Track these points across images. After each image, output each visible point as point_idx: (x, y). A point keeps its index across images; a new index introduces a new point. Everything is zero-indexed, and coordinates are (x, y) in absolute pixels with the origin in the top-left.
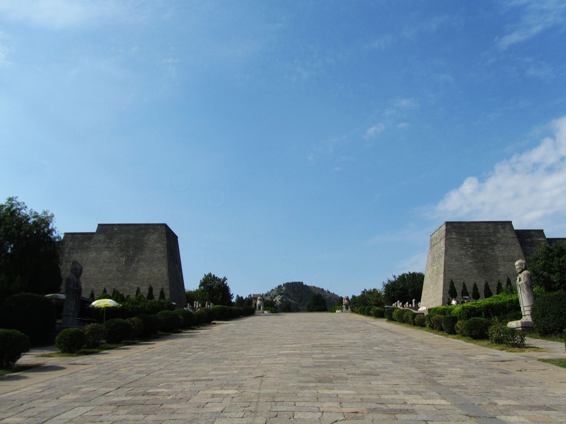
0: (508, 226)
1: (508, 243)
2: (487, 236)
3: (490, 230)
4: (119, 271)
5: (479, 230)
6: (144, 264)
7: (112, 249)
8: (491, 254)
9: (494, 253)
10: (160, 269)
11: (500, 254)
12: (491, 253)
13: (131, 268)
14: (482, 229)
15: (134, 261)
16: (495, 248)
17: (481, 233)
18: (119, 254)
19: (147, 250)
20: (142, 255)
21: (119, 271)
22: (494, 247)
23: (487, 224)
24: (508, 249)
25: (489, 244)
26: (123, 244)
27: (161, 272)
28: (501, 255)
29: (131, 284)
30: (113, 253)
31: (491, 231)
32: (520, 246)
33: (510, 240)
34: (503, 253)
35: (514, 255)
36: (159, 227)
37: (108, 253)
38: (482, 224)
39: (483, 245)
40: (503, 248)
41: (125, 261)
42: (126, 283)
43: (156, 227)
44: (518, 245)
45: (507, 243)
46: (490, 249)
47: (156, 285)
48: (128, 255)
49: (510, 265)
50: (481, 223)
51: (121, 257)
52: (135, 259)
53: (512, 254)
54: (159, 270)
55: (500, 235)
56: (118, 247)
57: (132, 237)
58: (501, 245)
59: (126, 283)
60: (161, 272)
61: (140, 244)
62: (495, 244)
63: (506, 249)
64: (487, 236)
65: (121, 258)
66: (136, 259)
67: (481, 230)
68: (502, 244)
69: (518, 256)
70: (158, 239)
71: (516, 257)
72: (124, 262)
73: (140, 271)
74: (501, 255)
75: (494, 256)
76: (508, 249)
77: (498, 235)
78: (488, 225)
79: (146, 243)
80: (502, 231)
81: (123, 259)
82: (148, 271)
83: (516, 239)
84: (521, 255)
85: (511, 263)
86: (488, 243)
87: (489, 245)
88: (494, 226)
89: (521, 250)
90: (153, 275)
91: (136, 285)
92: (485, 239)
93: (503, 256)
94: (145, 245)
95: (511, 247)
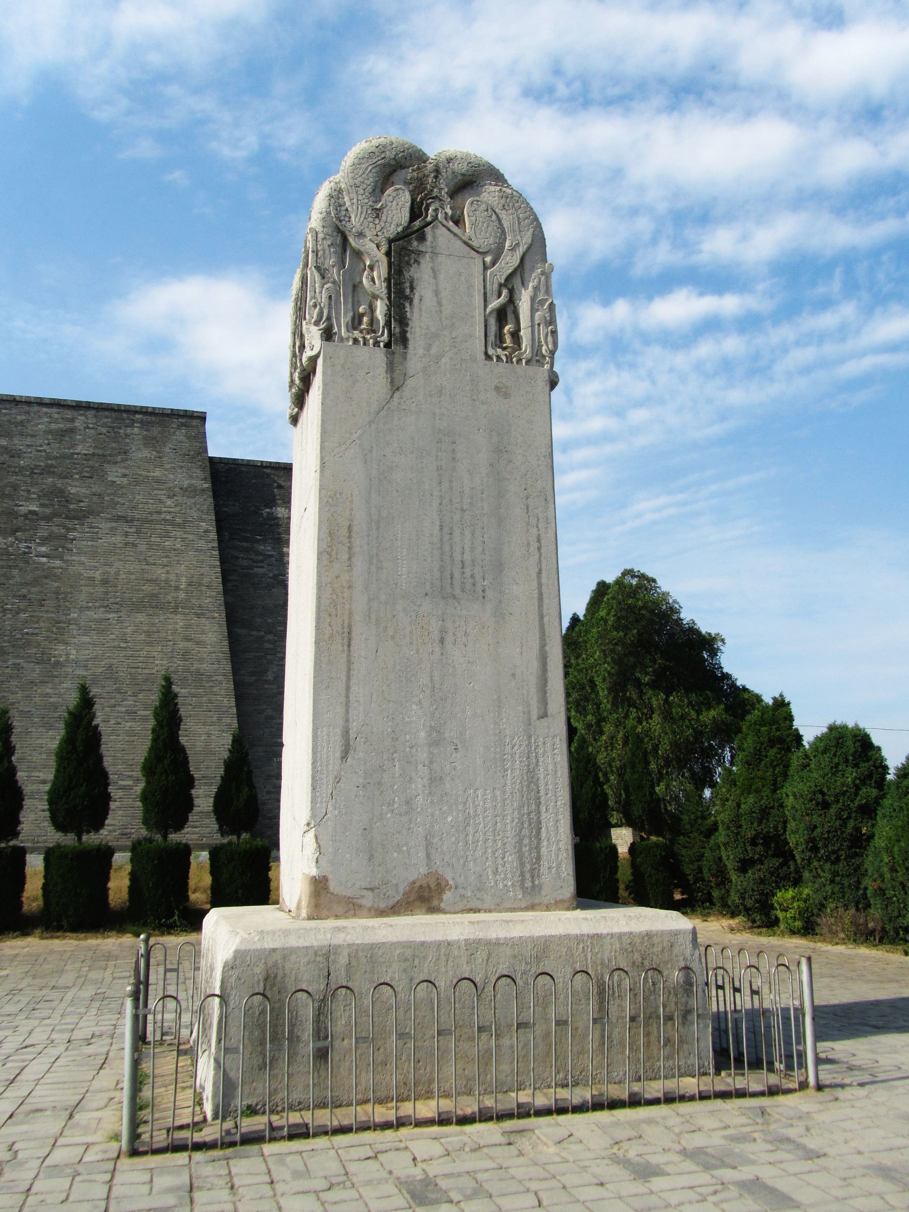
0: (180, 435)
1: (155, 517)
2: (48, 470)
3: (73, 446)
5: (16, 441)
8: (44, 564)
9: (58, 563)
11: (96, 568)
12: (44, 560)
14: (33, 436)
16: (71, 535)
17: (19, 455)
22: (68, 530)
23: (69, 414)
24: (142, 548)
25: (48, 511)
28: (98, 575)
31: (79, 449)
32: (213, 535)
33: (169, 502)
34: (111, 566)
35: (172, 577)
38: (45, 410)
39: (12, 514)
40: (118, 539)
44: (207, 531)
45: (150, 513)
46: (45, 541)
49: (129, 630)
50: (36, 408)
53: (160, 573)
55: (124, 476)
58: (114, 524)
62: (81, 516)
63: (134, 545)
64: (48, 470)
67: (29, 441)
68: (118, 518)
69: (190, 584)
71: (177, 589)
74: (98, 575)
75: (58, 578)
76: (142, 548)
77: (114, 474)
78: (73, 420)
80: (140, 453)
83: (208, 502)
84: (206, 580)
85: (141, 617)
86: (42, 505)
87: (47, 519)
88: (104, 430)
89: (216, 553)
92: (32, 484)
93: (105, 582)
95: (166, 535)
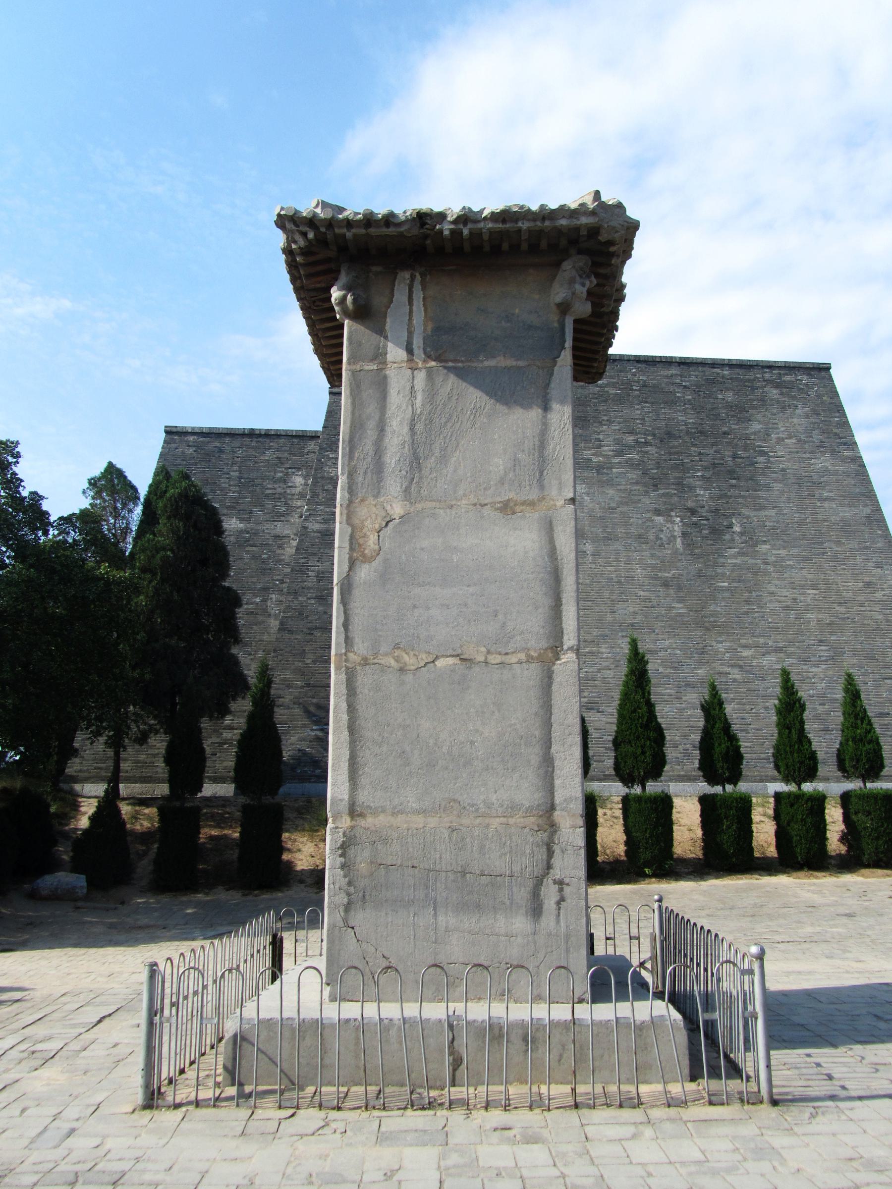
4: (666, 584)
6: (783, 552)
7: (598, 473)
10: (867, 579)
13: (720, 570)
15: (727, 537)
18: (646, 501)
19: (777, 486)
20: (762, 508)
21: (666, 584)
26: (652, 450)
27: (879, 595)
29: (746, 653)
30: (611, 492)
36: (805, 379)
37: (588, 494)
41: (684, 535)
42: (721, 648)
43: (788, 378)
47: (873, 658)
48: (690, 504)
51: (658, 512)
52: (730, 526)
54: (868, 584)
56: (632, 465)
57: (685, 418)
59: (721, 648)
60: (879, 595)
61: (735, 456)
65: (660, 519)
66: (737, 528)
70: (817, 436)
72: (679, 540)
73: (773, 589)
79: (763, 453)
81: (673, 522)
82: (814, 586)
90: (842, 609)
91: (772, 658)
94: (760, 459)
